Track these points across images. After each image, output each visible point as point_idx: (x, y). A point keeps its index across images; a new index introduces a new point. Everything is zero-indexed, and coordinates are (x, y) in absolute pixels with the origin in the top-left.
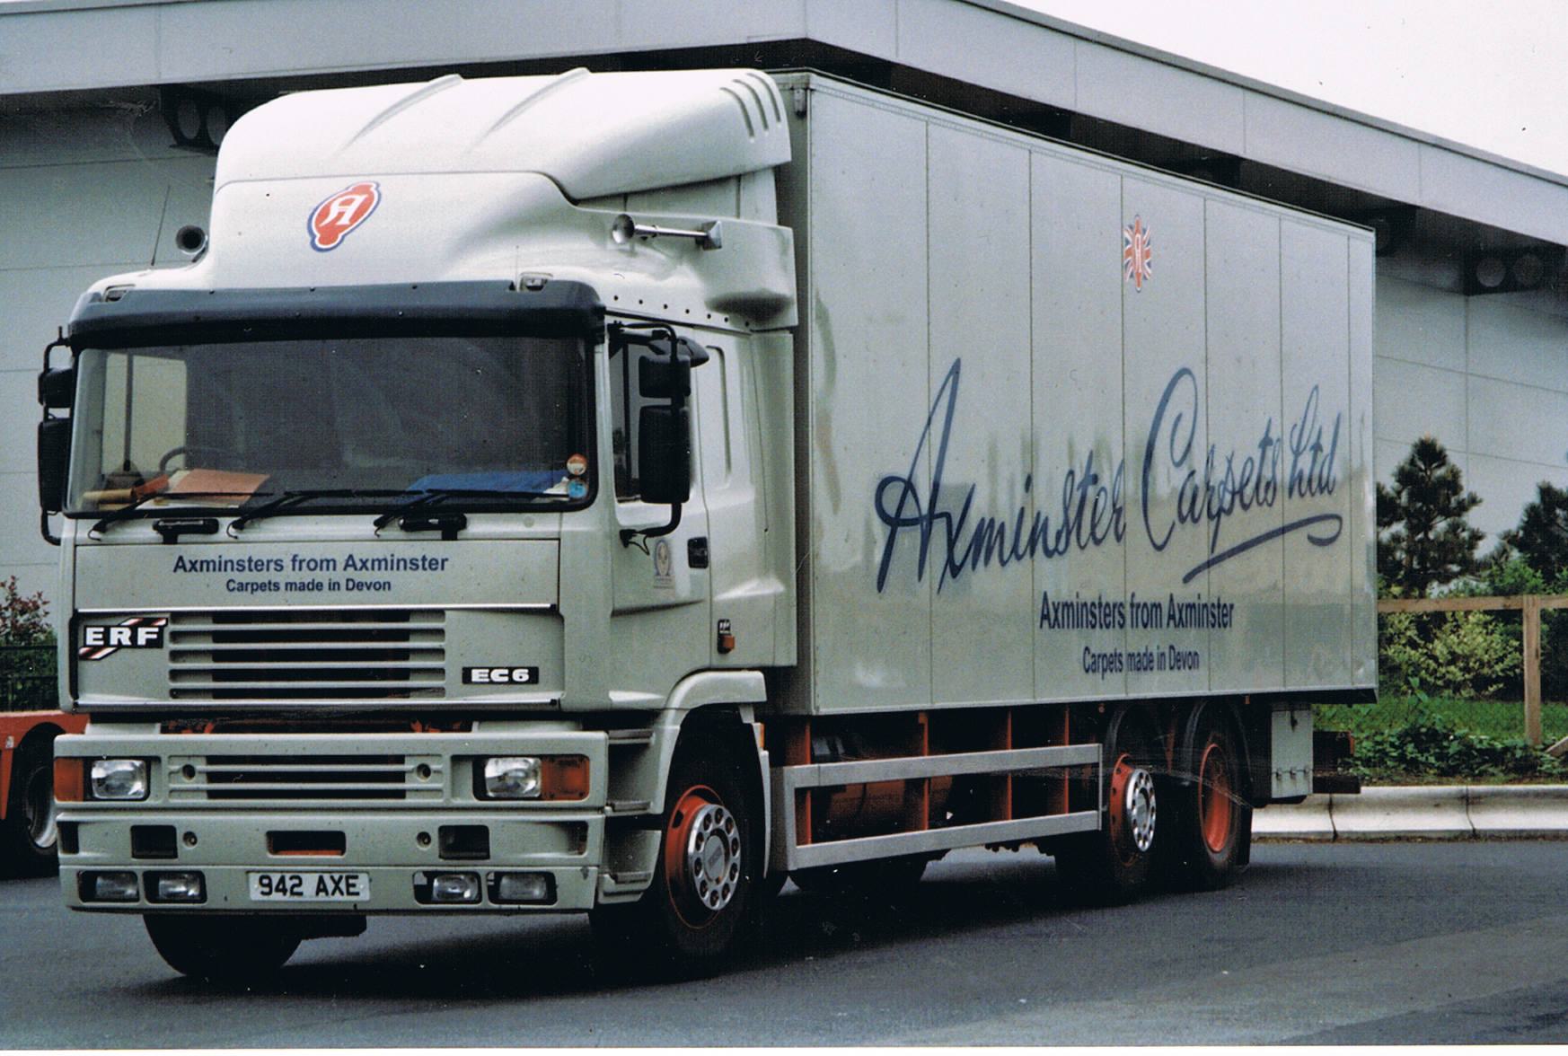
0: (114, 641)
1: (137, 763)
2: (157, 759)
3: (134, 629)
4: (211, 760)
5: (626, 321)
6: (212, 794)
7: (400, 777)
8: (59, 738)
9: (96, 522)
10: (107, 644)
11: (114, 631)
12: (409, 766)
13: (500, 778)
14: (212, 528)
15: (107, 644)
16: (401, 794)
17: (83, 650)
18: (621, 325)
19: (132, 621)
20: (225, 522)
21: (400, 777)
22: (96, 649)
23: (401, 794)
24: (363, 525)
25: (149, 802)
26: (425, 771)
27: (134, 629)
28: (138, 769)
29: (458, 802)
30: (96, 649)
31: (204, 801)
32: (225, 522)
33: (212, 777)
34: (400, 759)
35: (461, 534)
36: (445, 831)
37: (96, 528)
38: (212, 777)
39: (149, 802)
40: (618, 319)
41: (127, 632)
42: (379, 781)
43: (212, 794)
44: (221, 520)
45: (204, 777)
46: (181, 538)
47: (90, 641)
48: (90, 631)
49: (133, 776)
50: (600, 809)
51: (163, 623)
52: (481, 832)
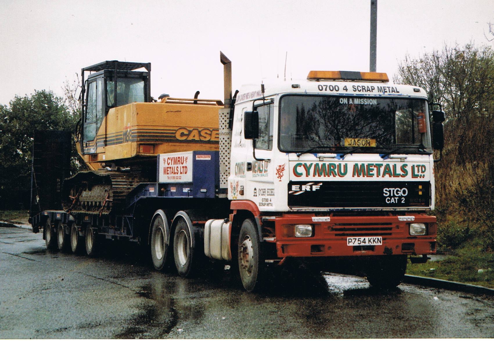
6: (336, 235)
7: (390, 229)
10: (301, 190)
12: (393, 226)
16: (390, 234)
17: (290, 192)
19: (310, 184)
21: (390, 229)
22: (296, 192)
23: (390, 234)
25: (314, 238)
26: (398, 227)
27: (311, 186)
31: (334, 237)
34: (391, 224)
41: (309, 187)
51: (321, 184)
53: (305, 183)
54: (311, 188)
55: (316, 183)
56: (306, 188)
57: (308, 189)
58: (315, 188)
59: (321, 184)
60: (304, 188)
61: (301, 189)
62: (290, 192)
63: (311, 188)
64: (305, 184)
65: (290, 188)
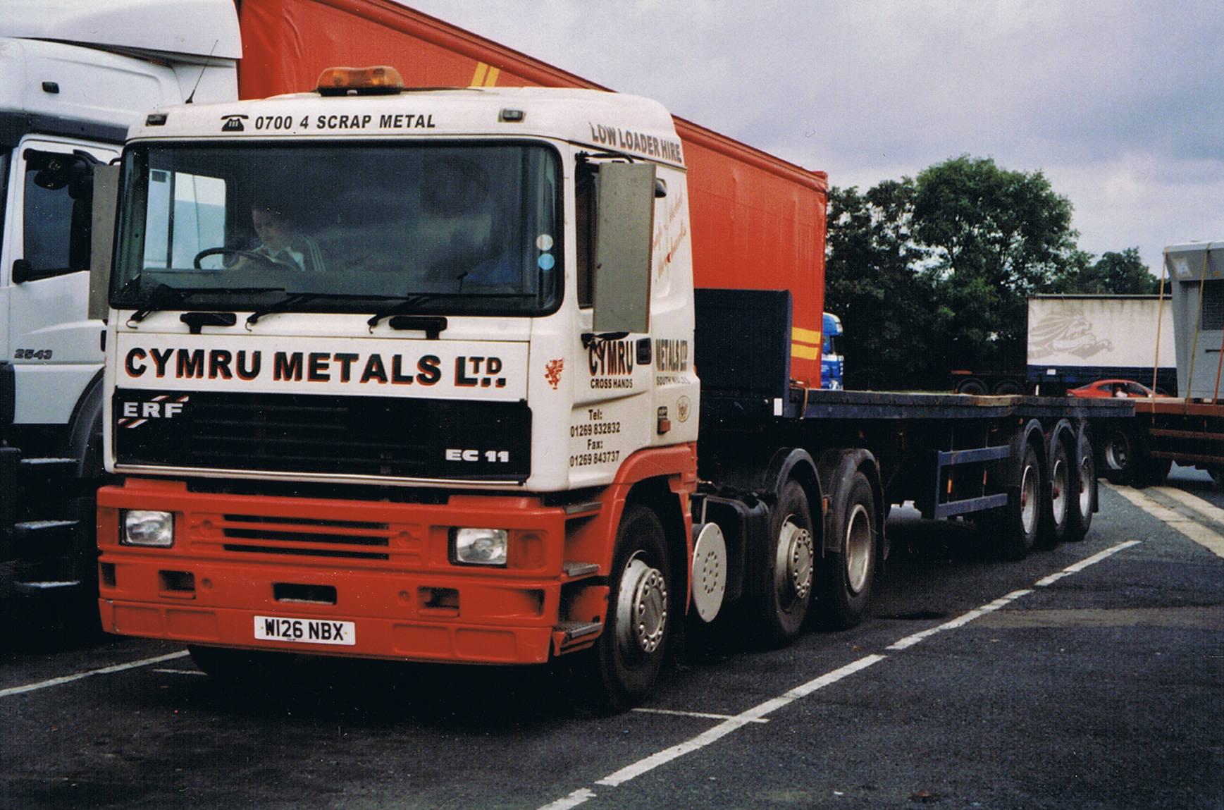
0: (146, 414)
1: (166, 514)
2: (181, 513)
4: (229, 517)
5: (591, 152)
6: (229, 547)
8: (101, 490)
9: (134, 312)
10: (141, 417)
11: (146, 406)
13: (471, 547)
14: (232, 321)
15: (141, 417)
16: (386, 557)
17: (121, 421)
18: (586, 155)
20: (242, 317)
22: (132, 420)
23: (386, 557)
24: (359, 322)
27: (162, 404)
28: (166, 519)
29: (433, 565)
30: (132, 420)
32: (242, 317)
33: (229, 533)
35: (442, 334)
36: (423, 589)
37: (133, 318)
38: (229, 533)
39: (175, 550)
40: (585, 150)
41: (156, 407)
42: (366, 543)
43: (229, 547)
44: (238, 314)
45: (222, 533)
46: (205, 329)
47: (126, 413)
48: (127, 405)
49: (162, 525)
50: (555, 578)
51: (186, 399)
52: (452, 593)
53: (147, 395)
54: (162, 411)
55: (173, 396)
56: (151, 409)
57: (156, 414)
58: (170, 410)
59: (186, 399)
60: (146, 406)
62: (121, 421)
63: (162, 411)
64: (149, 401)
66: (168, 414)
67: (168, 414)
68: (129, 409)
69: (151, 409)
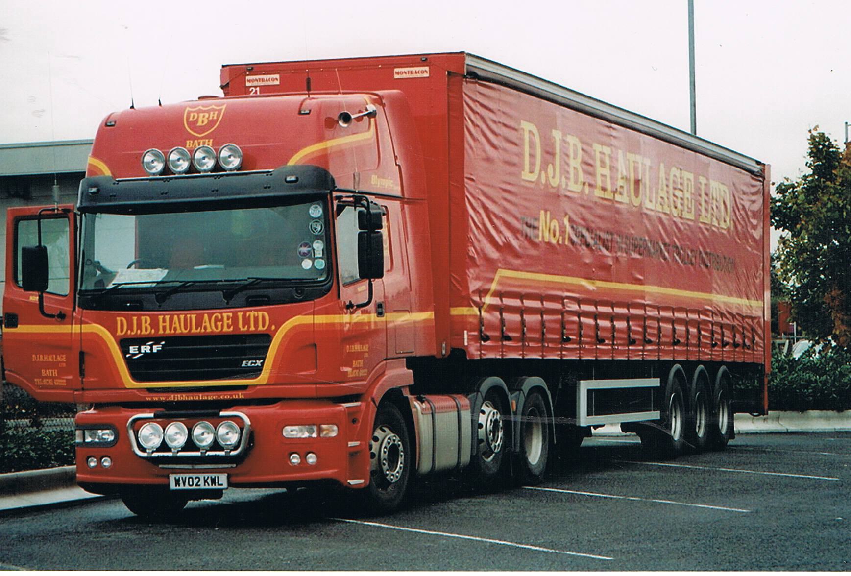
0: (143, 351)
3: (151, 346)
10: (140, 352)
11: (142, 347)
27: (151, 346)
47: (131, 351)
48: (131, 348)
54: (151, 349)
56: (146, 349)
57: (148, 351)
58: (155, 349)
60: (142, 347)
61: (139, 349)
63: (151, 349)
64: (145, 344)
65: (125, 351)
66: (155, 351)
67: (155, 351)
68: (133, 349)
69: (146, 349)
